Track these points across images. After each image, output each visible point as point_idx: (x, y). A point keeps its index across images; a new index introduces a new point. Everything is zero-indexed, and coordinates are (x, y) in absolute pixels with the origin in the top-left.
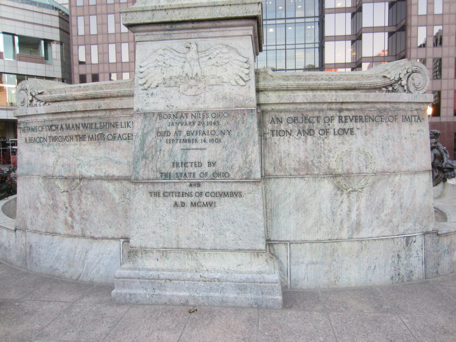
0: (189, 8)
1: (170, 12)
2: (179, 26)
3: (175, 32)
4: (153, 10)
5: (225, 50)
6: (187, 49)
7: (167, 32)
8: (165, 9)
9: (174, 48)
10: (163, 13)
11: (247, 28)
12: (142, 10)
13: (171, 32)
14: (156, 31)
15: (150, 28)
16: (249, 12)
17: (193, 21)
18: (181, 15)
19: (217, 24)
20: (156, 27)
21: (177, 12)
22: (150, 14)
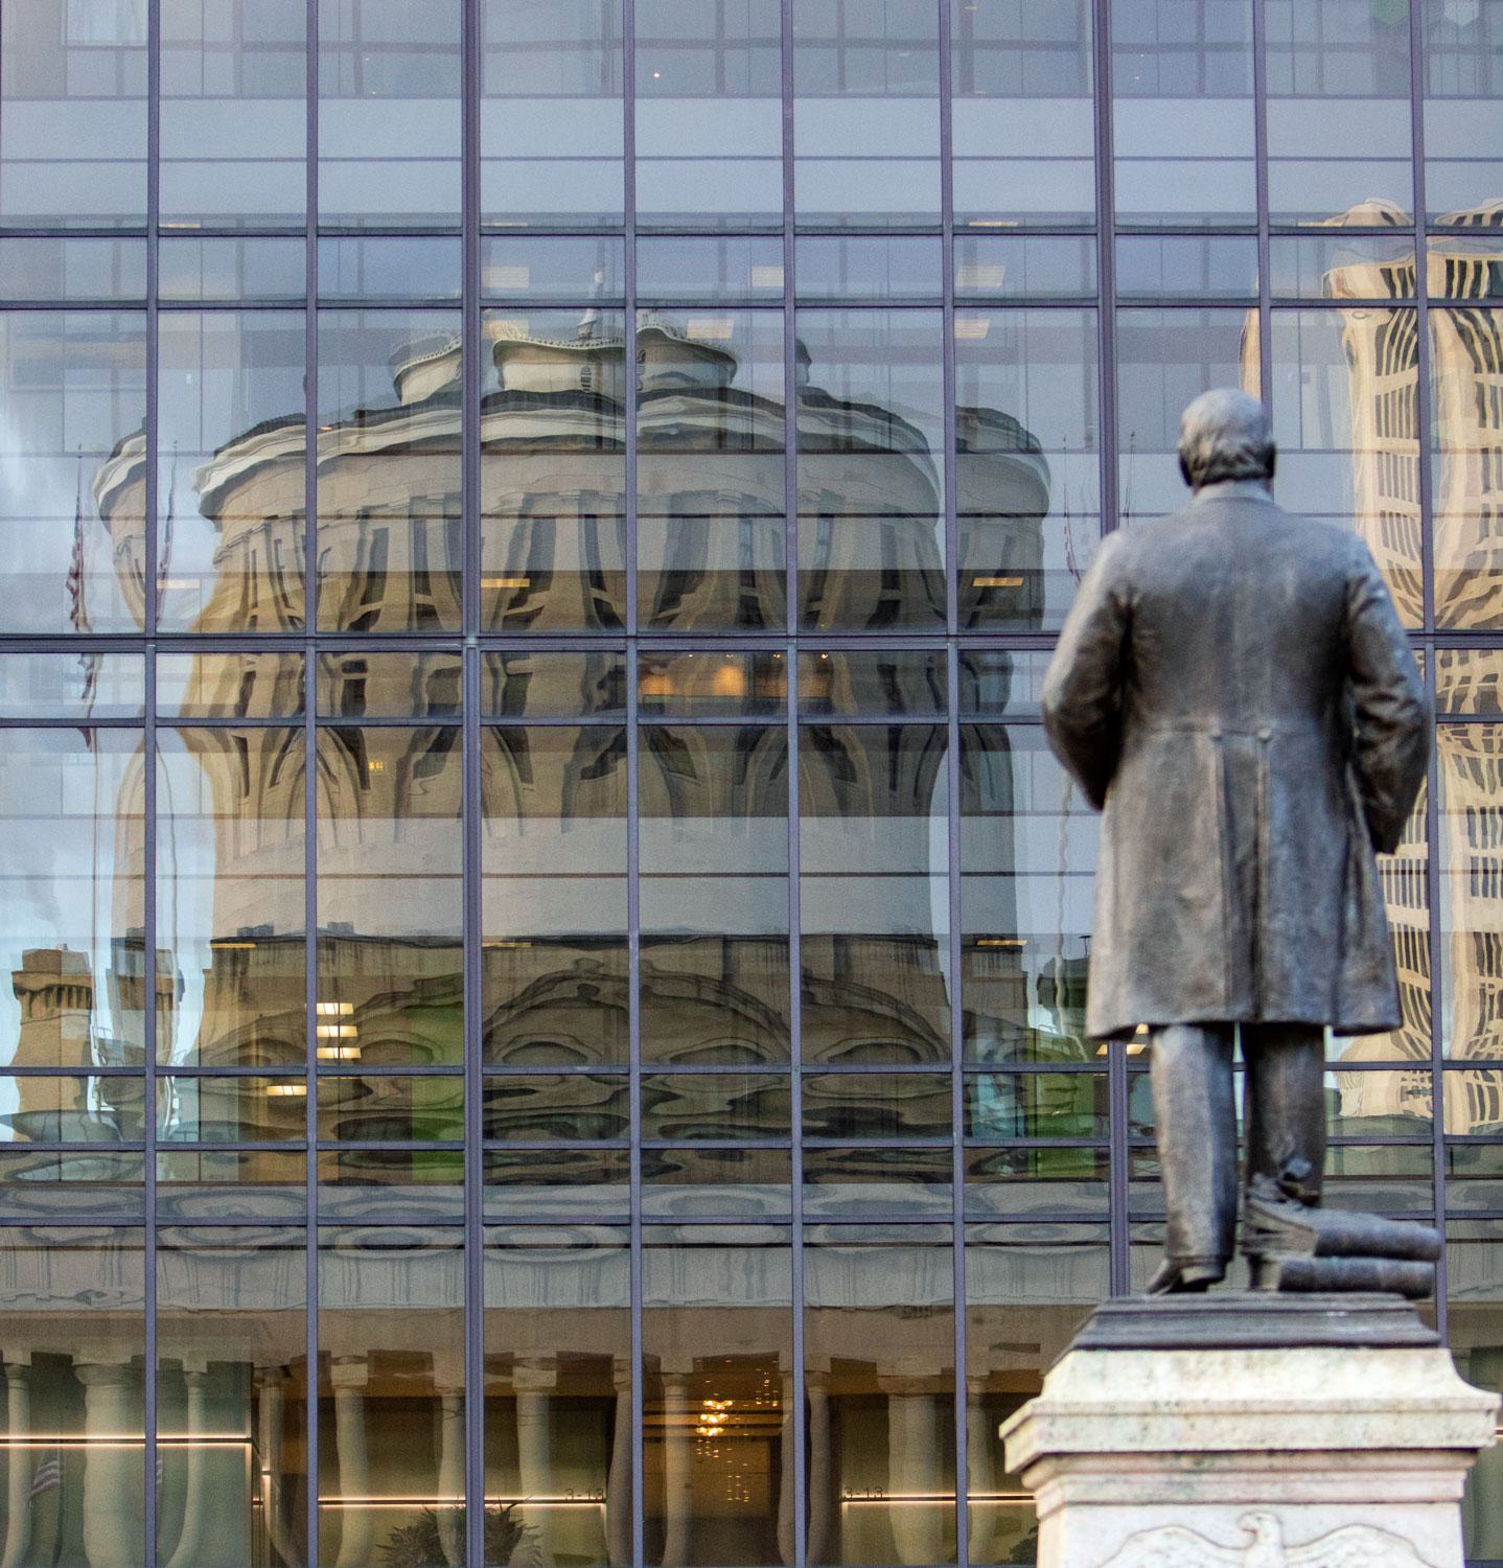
0: (1265, 1413)
1: (1203, 1424)
2: (1224, 1463)
3: (1205, 1477)
4: (1145, 1414)
5: (1375, 1544)
6: (1246, 1536)
7: (1177, 1478)
8: (1187, 1415)
9: (1200, 1528)
10: (1180, 1424)
11: (1446, 1475)
12: (1108, 1410)
13: (1193, 1478)
14: (1143, 1471)
15: (1123, 1464)
16: (1459, 1437)
17: (1271, 1452)
18: (1238, 1434)
19: (1352, 1461)
20: (1145, 1463)
21: (1225, 1423)
22: (1133, 1425)
